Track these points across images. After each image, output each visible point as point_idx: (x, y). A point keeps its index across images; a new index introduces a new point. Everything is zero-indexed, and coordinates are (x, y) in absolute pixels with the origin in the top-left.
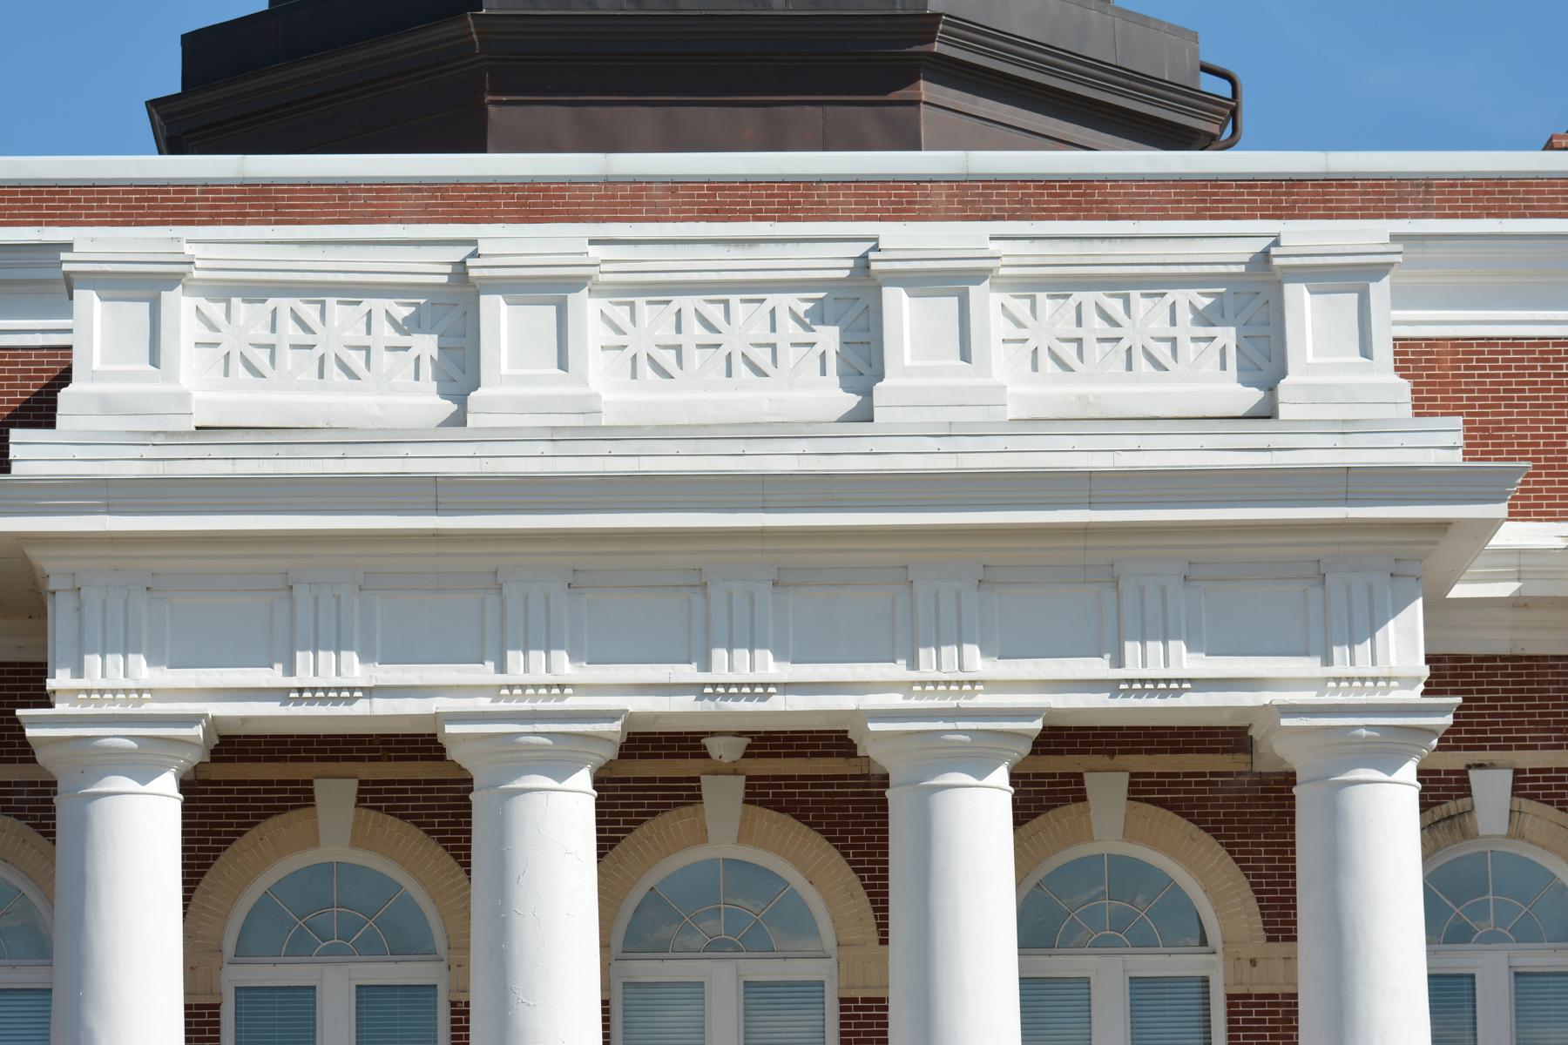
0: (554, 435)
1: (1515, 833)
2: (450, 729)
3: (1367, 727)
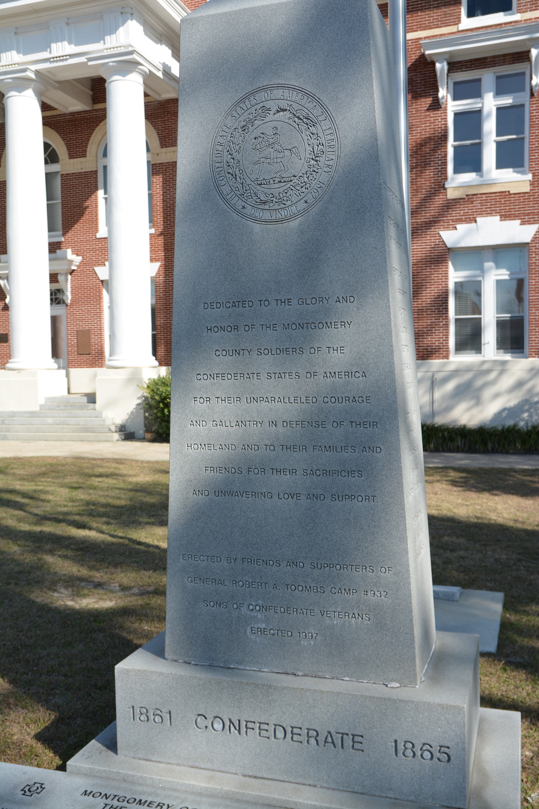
3: (112, 62)
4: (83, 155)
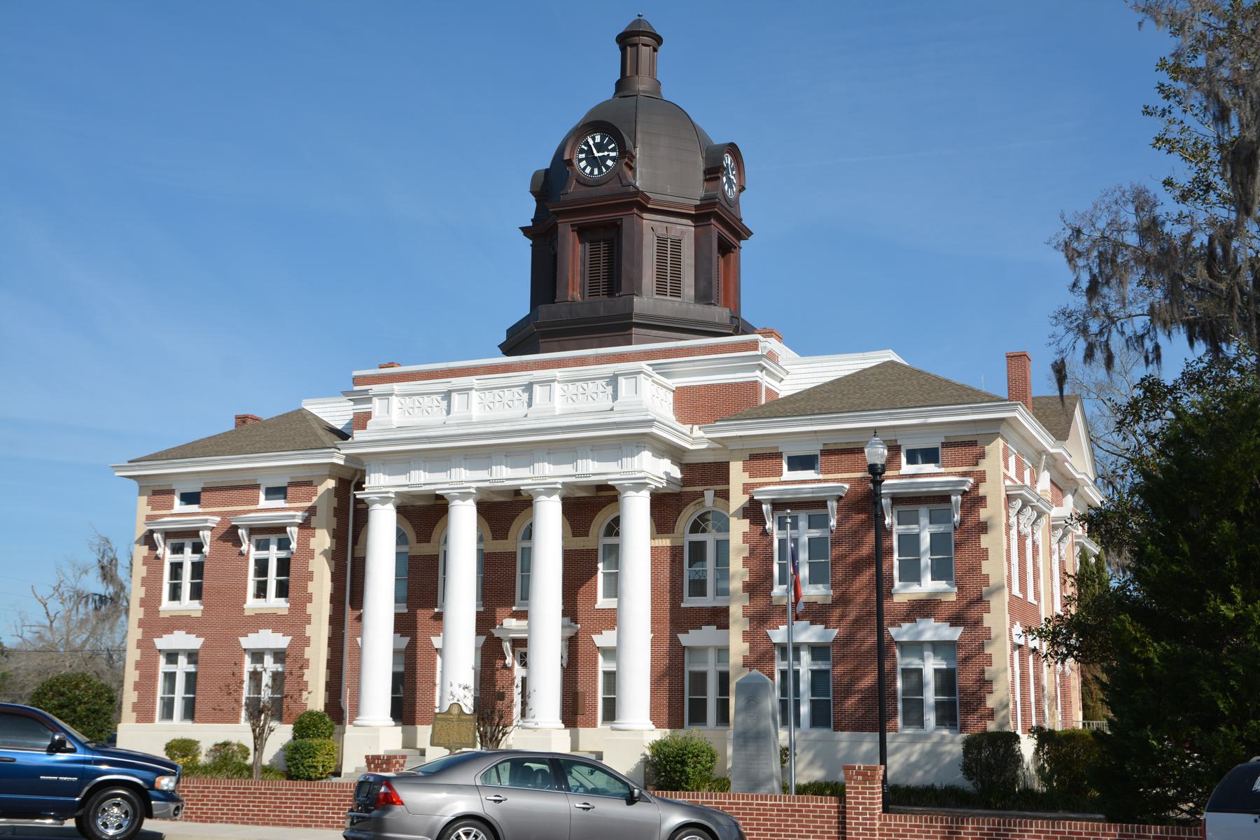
0: (458, 425)
1: (715, 506)
2: (522, 488)
4: (586, 534)
